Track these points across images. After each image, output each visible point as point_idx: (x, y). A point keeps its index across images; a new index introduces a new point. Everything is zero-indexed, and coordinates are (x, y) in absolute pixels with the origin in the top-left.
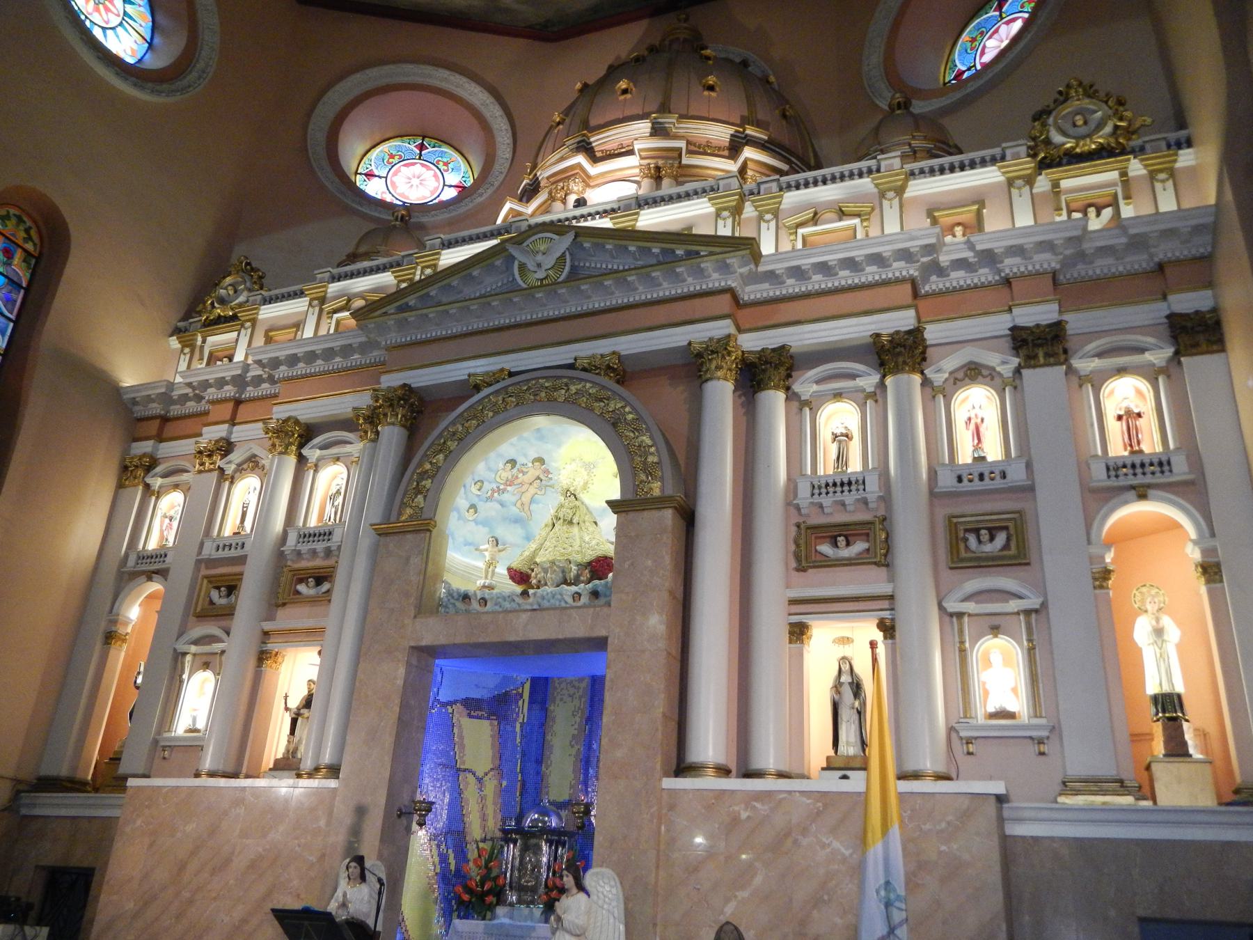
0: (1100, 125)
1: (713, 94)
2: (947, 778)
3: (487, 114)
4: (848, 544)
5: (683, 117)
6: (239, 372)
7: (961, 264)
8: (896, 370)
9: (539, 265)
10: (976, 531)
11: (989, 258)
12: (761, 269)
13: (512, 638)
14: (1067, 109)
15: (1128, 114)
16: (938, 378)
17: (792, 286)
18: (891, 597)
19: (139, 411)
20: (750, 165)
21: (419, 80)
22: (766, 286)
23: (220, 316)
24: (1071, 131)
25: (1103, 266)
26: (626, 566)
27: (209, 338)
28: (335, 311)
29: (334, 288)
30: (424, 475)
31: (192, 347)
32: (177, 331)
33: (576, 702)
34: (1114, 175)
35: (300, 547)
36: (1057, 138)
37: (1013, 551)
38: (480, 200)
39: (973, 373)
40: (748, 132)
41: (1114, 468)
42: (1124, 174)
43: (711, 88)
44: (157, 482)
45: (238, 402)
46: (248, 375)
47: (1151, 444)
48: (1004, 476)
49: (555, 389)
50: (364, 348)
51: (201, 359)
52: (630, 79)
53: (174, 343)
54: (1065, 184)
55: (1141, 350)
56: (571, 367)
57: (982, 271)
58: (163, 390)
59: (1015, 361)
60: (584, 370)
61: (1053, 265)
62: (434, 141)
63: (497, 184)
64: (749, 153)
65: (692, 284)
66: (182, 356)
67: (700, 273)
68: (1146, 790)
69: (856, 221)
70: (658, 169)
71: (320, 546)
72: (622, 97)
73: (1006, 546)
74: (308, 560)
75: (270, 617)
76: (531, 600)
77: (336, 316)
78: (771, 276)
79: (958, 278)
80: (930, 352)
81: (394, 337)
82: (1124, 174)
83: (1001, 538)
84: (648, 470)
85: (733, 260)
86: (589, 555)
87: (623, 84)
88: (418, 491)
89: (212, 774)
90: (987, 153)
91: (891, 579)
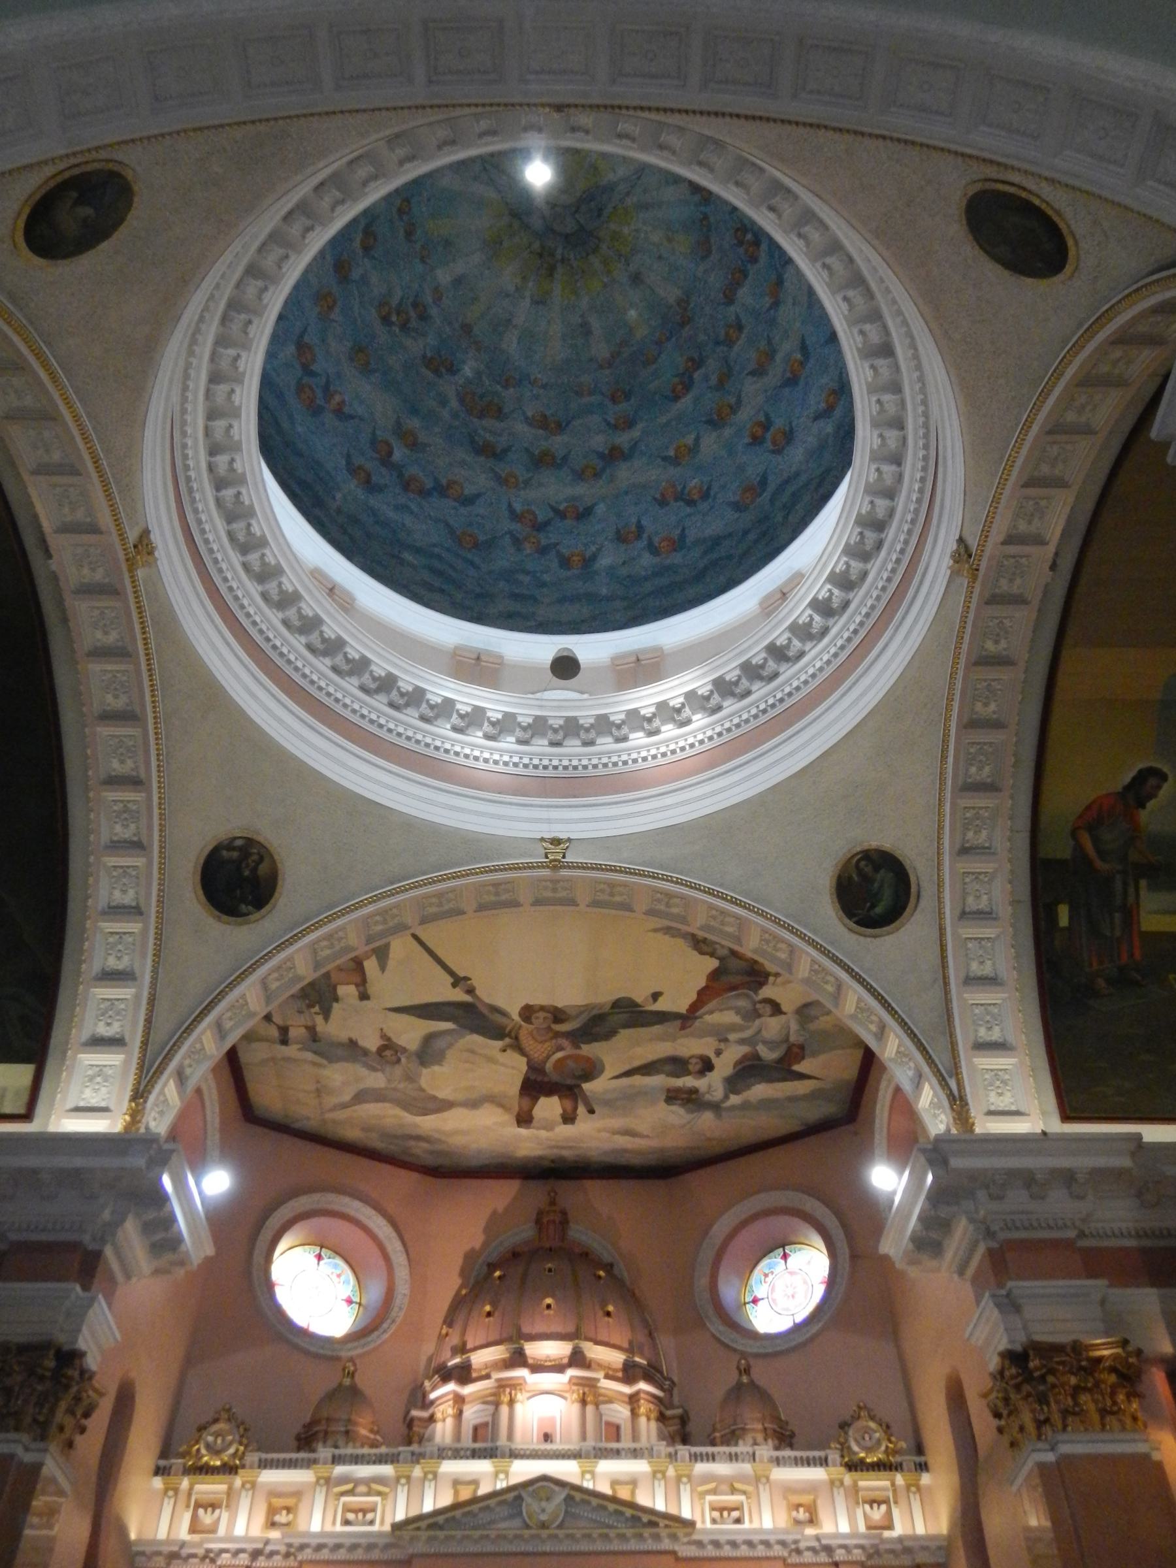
0: (879, 1442)
1: (610, 1320)
3: (389, 1249)
5: (597, 1343)
6: (260, 1546)
7: (812, 1549)
11: (828, 1549)
12: (695, 1537)
15: (893, 1439)
17: (710, 1551)
20: (642, 1395)
21: (336, 1207)
22: (693, 1548)
23: (207, 1464)
24: (862, 1442)
27: (198, 1487)
28: (343, 1494)
29: (340, 1470)
31: (176, 1491)
32: (158, 1471)
34: (887, 1483)
36: (855, 1448)
38: (386, 1336)
40: (637, 1359)
42: (893, 1484)
43: (608, 1314)
50: (387, 1546)
51: (188, 1506)
52: (553, 1297)
53: (158, 1483)
54: (862, 1484)
58: (175, 1549)
61: (863, 1559)
62: (329, 1252)
63: (399, 1320)
64: (643, 1386)
65: (650, 1545)
66: (166, 1500)
67: (657, 1537)
69: (742, 1498)
70: (584, 1394)
72: (547, 1312)
77: (344, 1499)
78: (700, 1544)
81: (420, 1547)
82: (893, 1484)
85: (680, 1533)
87: (549, 1301)
90: (817, 1454)
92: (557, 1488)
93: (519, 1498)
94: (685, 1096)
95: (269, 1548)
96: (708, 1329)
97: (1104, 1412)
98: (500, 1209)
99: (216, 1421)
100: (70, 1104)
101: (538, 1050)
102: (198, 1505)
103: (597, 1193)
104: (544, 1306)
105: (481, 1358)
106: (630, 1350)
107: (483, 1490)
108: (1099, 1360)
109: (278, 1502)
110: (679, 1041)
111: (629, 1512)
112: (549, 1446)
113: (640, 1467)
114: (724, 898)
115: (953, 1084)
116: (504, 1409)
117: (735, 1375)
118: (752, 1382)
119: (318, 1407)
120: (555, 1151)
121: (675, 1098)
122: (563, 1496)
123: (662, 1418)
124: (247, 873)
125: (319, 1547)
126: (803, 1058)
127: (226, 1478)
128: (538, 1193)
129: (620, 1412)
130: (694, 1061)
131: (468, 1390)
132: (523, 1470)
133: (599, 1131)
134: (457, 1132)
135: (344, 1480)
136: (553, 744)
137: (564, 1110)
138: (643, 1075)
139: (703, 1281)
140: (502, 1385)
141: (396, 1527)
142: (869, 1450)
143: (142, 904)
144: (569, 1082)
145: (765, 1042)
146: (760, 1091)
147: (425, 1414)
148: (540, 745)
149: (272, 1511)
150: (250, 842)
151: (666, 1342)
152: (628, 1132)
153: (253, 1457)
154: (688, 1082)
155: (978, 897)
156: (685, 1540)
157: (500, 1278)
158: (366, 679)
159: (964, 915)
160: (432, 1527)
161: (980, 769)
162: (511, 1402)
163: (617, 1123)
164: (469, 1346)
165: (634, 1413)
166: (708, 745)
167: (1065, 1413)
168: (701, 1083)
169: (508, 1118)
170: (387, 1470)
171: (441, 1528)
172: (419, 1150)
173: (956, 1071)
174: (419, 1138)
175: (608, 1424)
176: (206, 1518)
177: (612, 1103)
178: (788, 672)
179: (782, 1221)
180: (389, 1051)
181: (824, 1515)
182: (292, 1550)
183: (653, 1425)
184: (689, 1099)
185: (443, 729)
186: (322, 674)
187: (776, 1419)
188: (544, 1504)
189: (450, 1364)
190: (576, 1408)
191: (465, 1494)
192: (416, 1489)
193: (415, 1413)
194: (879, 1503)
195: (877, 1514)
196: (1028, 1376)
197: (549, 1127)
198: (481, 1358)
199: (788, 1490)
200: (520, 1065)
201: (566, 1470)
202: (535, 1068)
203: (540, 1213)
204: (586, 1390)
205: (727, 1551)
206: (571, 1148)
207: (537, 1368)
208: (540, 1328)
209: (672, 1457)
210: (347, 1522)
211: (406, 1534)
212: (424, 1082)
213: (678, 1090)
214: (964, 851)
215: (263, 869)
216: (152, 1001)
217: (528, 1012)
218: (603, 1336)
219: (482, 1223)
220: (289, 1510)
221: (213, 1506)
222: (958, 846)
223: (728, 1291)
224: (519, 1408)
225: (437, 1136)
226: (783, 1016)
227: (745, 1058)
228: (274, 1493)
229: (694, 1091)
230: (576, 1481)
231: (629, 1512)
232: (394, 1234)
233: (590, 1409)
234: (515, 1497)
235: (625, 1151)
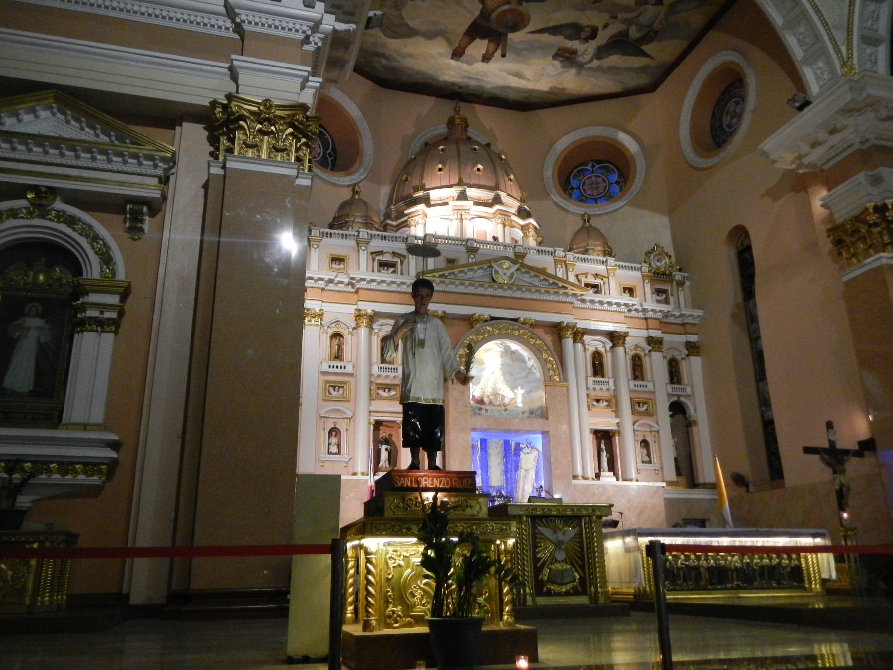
2: (637, 481)
4: (603, 402)
6: (333, 278)
7: (636, 310)
9: (505, 274)
10: (639, 404)
12: (583, 297)
13: (514, 429)
18: (618, 423)
22: (580, 302)
25: (671, 320)
26: (552, 405)
33: (498, 449)
35: (380, 373)
37: (649, 412)
40: (526, 207)
43: (510, 180)
45: (323, 289)
46: (336, 279)
48: (646, 386)
56: (516, 320)
57: (641, 313)
59: (650, 348)
60: (523, 323)
67: (566, 294)
71: (392, 374)
72: (478, 172)
73: (647, 410)
74: (383, 379)
75: (370, 405)
76: (507, 412)
78: (584, 301)
79: (633, 313)
83: (646, 407)
87: (480, 166)
89: (363, 474)
91: (617, 417)
92: (512, 264)
94: (567, 55)
95: (337, 280)
96: (552, 199)
104: (475, 169)
106: (522, 200)
110: (588, 13)
111: (551, 281)
115: (844, 49)
117: (582, 222)
120: (466, 80)
121: (561, 56)
126: (652, 41)
128: (446, 108)
130: (586, 29)
133: (501, 70)
134: (410, 55)
137: (487, 51)
138: (550, 34)
144: (501, 30)
145: (637, 25)
146: (614, 60)
147: (394, 223)
152: (519, 75)
156: (580, 298)
157: (442, 150)
160: (440, 276)
163: (514, 66)
164: (427, 187)
169: (450, 51)
171: (446, 277)
174: (384, 56)
182: (354, 282)
188: (505, 271)
189: (414, 196)
190: (500, 227)
193: (389, 222)
197: (470, 63)
198: (434, 194)
202: (484, 15)
204: (506, 217)
206: (478, 80)
207: (476, 204)
212: (404, 14)
213: (566, 50)
225: (395, 56)
226: (660, 7)
227: (619, 33)
229: (575, 52)
233: (507, 228)
235: (510, 88)
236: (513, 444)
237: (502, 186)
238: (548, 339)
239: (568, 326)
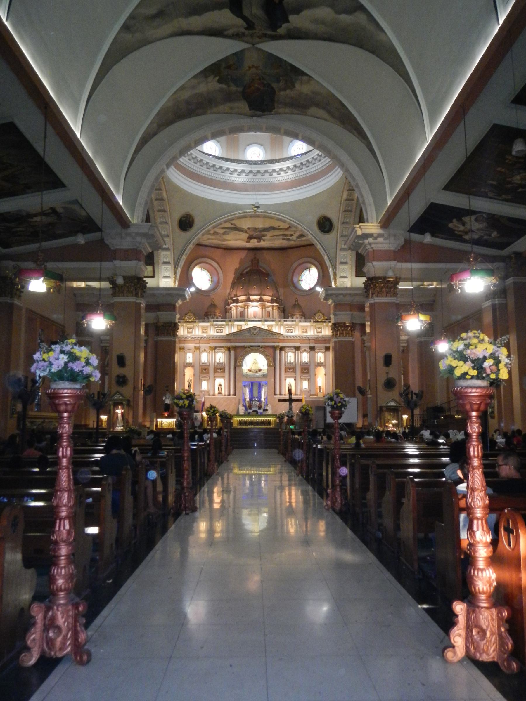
0: (321, 317)
2: (300, 395)
3: (218, 270)
5: (265, 295)
8: (297, 350)
11: (308, 338)
14: (318, 314)
16: (301, 351)
17: (286, 338)
19: (180, 339)
25: (319, 339)
29: (215, 323)
30: (240, 359)
31: (183, 326)
39: (305, 351)
41: (318, 363)
44: (186, 351)
47: (322, 361)
49: (258, 349)
50: (225, 337)
55: (322, 350)
56: (259, 346)
64: (275, 304)
65: (275, 338)
67: (276, 337)
68: (317, 395)
71: (221, 365)
78: (284, 337)
79: (305, 339)
80: (301, 348)
81: (232, 338)
84: (271, 362)
86: (259, 369)
88: (240, 361)
89: (212, 395)
93: (250, 330)
97: (346, 334)
98: (243, 258)
99: (188, 313)
100: (163, 276)
101: (251, 233)
102: (188, 328)
103: (265, 253)
105: (241, 298)
106: (272, 296)
107: (243, 328)
108: (389, 281)
109: (203, 328)
112: (255, 319)
113: (273, 323)
114: (293, 221)
115: (335, 270)
116: (246, 310)
118: (298, 303)
119: (208, 309)
122: (258, 330)
123: (279, 308)
124: (187, 222)
125: (213, 337)
127: (192, 323)
129: (270, 309)
131: (238, 305)
132: (251, 324)
135: (216, 325)
136: (254, 176)
139: (290, 277)
140: (245, 305)
141: (227, 335)
142: (319, 319)
143: (169, 234)
148: (251, 176)
149: (203, 330)
150: (188, 215)
151: (281, 290)
153: (197, 320)
154: (288, 237)
155: (345, 232)
158: (208, 166)
159: (342, 236)
160: (234, 335)
161: (348, 207)
162: (248, 309)
163: (270, 243)
164: (238, 295)
165: (273, 309)
166: (292, 179)
167: (340, 334)
168: (291, 238)
170: (224, 323)
171: (236, 335)
172: (221, 246)
173: (335, 268)
175: (268, 312)
176: (190, 330)
177: (269, 240)
178: (311, 166)
179: (309, 265)
180: (215, 233)
181: (308, 331)
183: (277, 311)
184: (288, 240)
185: (227, 174)
186: (198, 167)
187: (303, 312)
190: (261, 310)
191: (240, 328)
192: (230, 328)
193: (227, 307)
194: (319, 328)
195: (319, 330)
196: (336, 327)
197: (253, 243)
198: (241, 298)
199: (302, 326)
200: (248, 235)
201: (258, 324)
203: (252, 260)
205: (289, 338)
207: (252, 301)
208: (253, 293)
209: (279, 321)
210: (217, 332)
211: (229, 336)
214: (343, 223)
215: (191, 220)
216: (174, 254)
217: (249, 228)
218: (266, 294)
219: (238, 261)
220: (205, 329)
221: (190, 328)
222: (342, 222)
223: (295, 280)
224: (249, 310)
228: (202, 327)
230: (261, 327)
231: (271, 332)
232: (218, 266)
234: (249, 329)
236: (262, 384)
237: (262, 293)
238: (271, 351)
239: (277, 347)
